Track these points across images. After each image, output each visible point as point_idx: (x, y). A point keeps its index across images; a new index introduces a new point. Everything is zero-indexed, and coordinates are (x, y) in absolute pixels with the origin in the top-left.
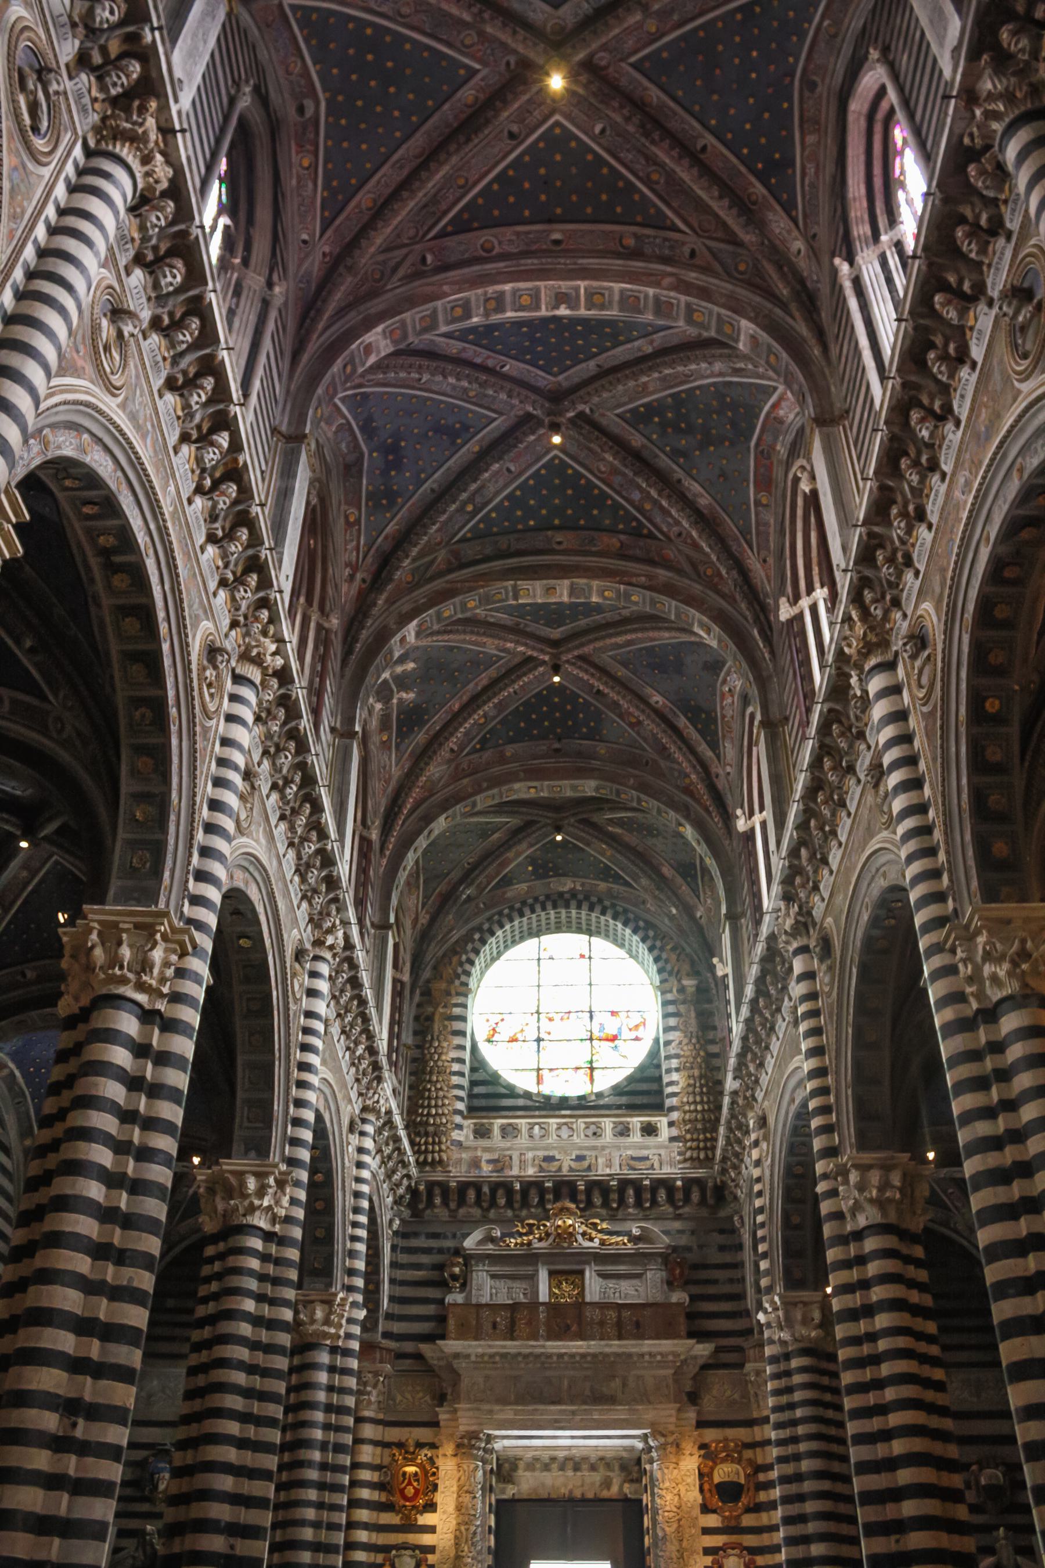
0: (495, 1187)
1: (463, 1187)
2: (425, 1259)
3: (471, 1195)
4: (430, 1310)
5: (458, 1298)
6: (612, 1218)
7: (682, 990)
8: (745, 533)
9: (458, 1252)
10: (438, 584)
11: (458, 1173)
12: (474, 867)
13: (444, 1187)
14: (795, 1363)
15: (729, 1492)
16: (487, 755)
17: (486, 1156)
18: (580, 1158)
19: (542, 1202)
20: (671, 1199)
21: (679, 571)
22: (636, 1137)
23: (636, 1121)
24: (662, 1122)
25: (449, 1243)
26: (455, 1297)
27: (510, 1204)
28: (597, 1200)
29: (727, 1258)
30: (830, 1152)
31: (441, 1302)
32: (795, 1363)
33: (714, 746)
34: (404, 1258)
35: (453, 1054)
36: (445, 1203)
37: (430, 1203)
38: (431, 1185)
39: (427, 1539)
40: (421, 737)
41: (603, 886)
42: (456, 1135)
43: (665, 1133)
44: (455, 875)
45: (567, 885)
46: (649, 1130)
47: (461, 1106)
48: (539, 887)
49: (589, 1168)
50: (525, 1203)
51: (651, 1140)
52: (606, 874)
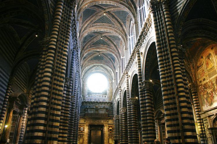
0: (90, 102)
1: (87, 102)
2: (83, 108)
3: (88, 103)
4: (84, 113)
5: (87, 112)
6: (101, 105)
7: (109, 83)
8: (119, 48)
9: (87, 108)
10: (89, 49)
11: (87, 101)
12: (89, 69)
13: (85, 102)
14: (117, 121)
15: (111, 130)
16: (92, 61)
17: (89, 99)
18: (99, 99)
19: (95, 103)
20: (107, 104)
21: (112, 50)
22: (104, 97)
23: (104, 96)
24: (106, 96)
25: (86, 107)
26: (87, 112)
27: (92, 104)
28: (100, 103)
29: (112, 109)
30: (121, 107)
31: (85, 113)
32: (117, 121)
33: (114, 62)
34: (81, 108)
35: (86, 88)
36: (85, 103)
37: (84, 103)
38: (84, 102)
39: (83, 133)
40: (85, 59)
41: (102, 71)
42: (86, 96)
43: (107, 97)
44: (87, 70)
45: (98, 71)
46: (105, 97)
47: (87, 94)
48: (95, 71)
49: (99, 100)
50: (93, 103)
51: (105, 98)
52: (103, 70)
